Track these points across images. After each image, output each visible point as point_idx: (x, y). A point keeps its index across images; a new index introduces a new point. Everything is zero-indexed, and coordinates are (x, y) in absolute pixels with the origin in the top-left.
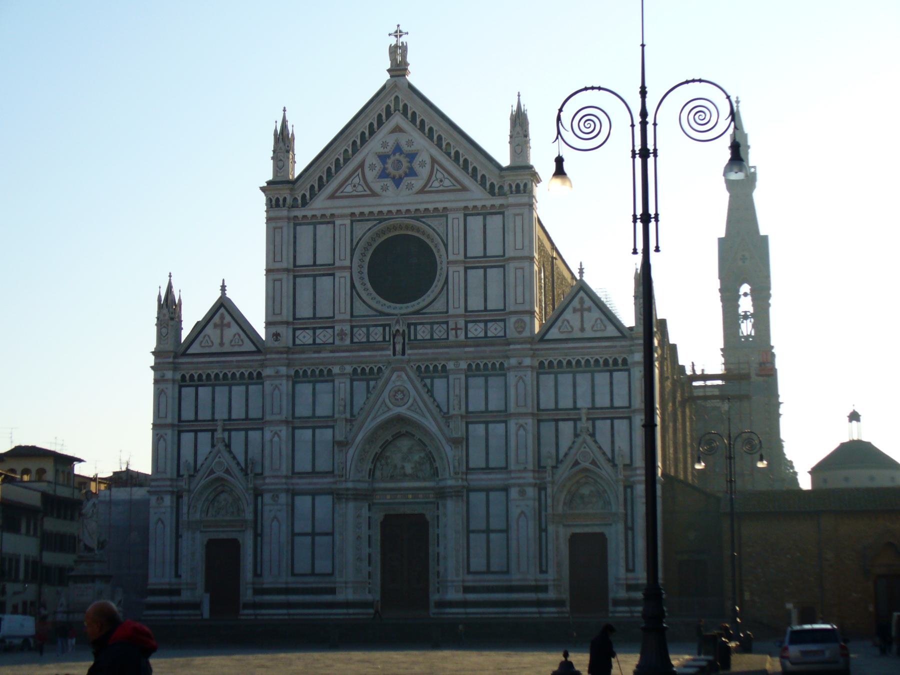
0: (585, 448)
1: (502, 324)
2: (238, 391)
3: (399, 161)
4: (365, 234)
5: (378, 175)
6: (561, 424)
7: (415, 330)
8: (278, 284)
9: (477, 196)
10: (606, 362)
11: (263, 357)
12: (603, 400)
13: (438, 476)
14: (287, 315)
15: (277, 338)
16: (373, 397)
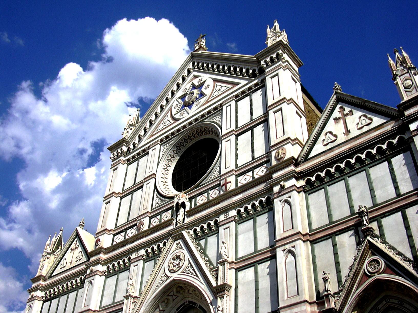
6: (339, 239)
7: (195, 200)
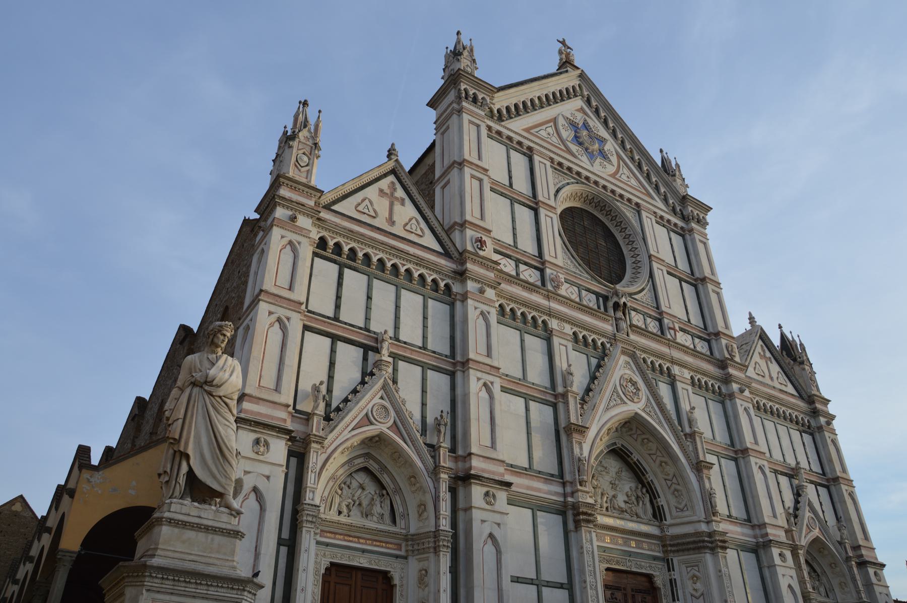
13: (666, 520)
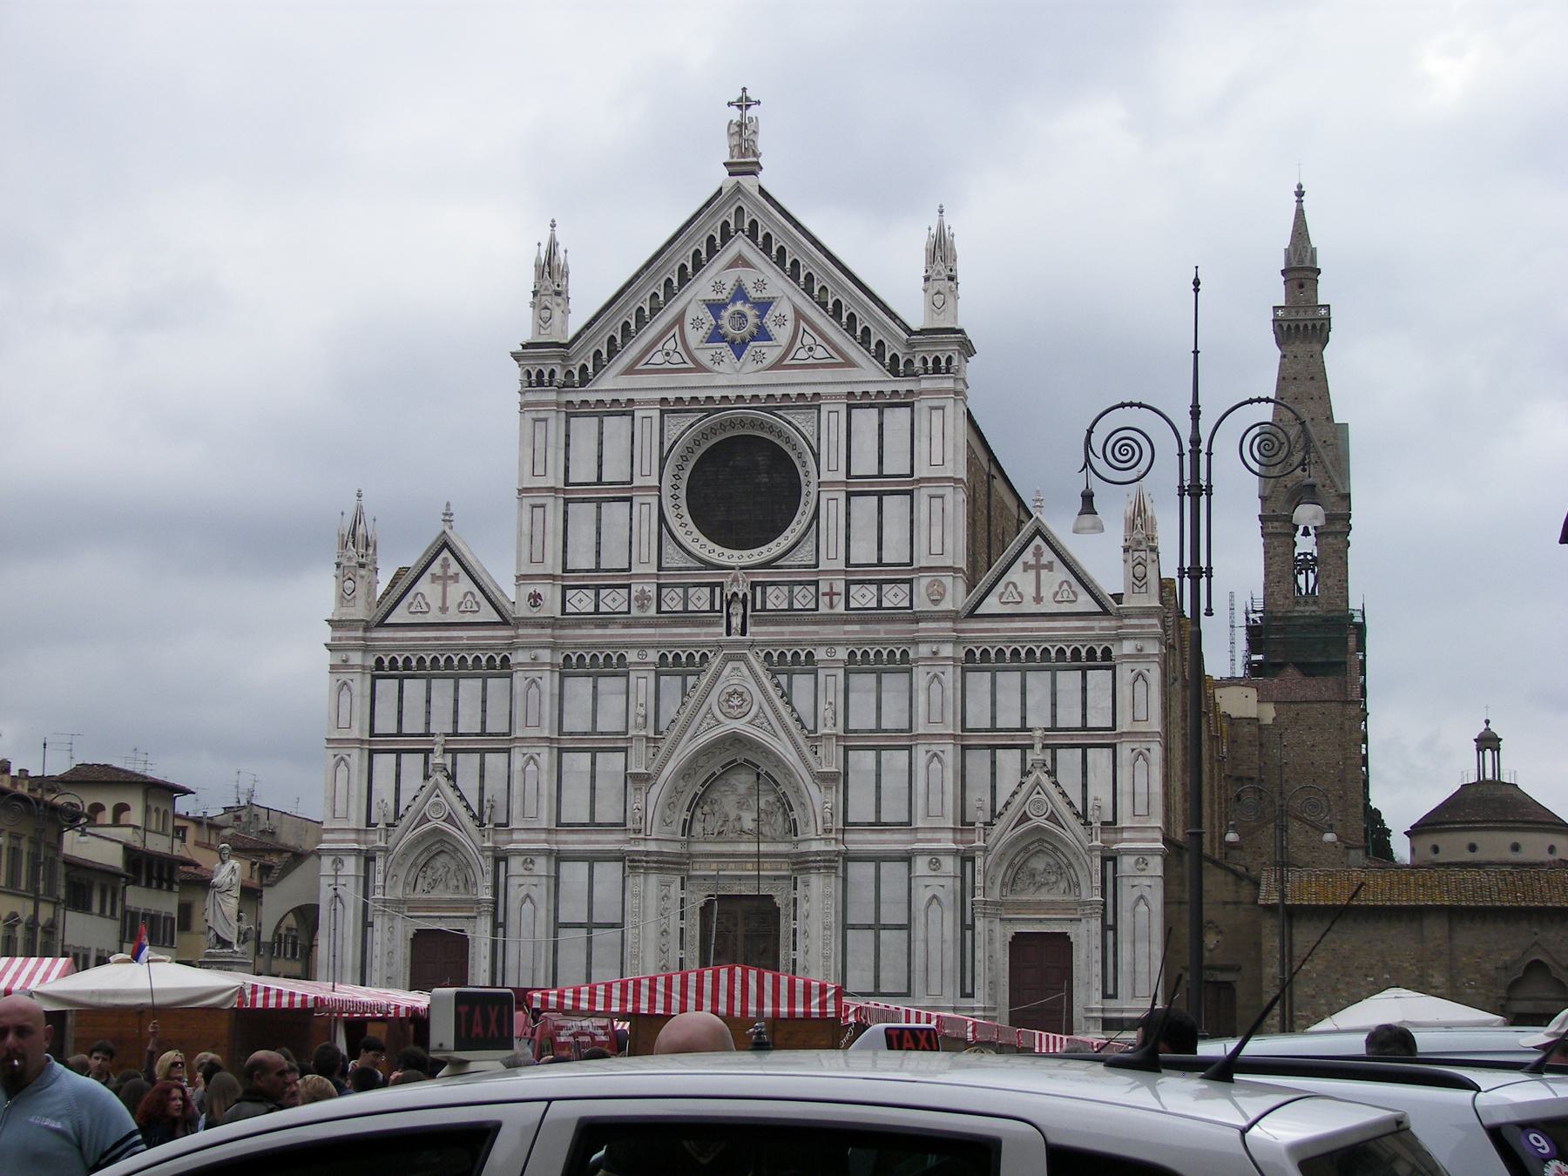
0: (1038, 793)
1: (906, 587)
2: (471, 688)
3: (742, 315)
4: (683, 433)
5: (707, 336)
7: (764, 593)
8: (538, 512)
9: (869, 375)
10: (1076, 652)
11: (512, 633)
12: (1069, 716)
13: (796, 835)
14: (552, 565)
15: (536, 601)
16: (691, 703)
